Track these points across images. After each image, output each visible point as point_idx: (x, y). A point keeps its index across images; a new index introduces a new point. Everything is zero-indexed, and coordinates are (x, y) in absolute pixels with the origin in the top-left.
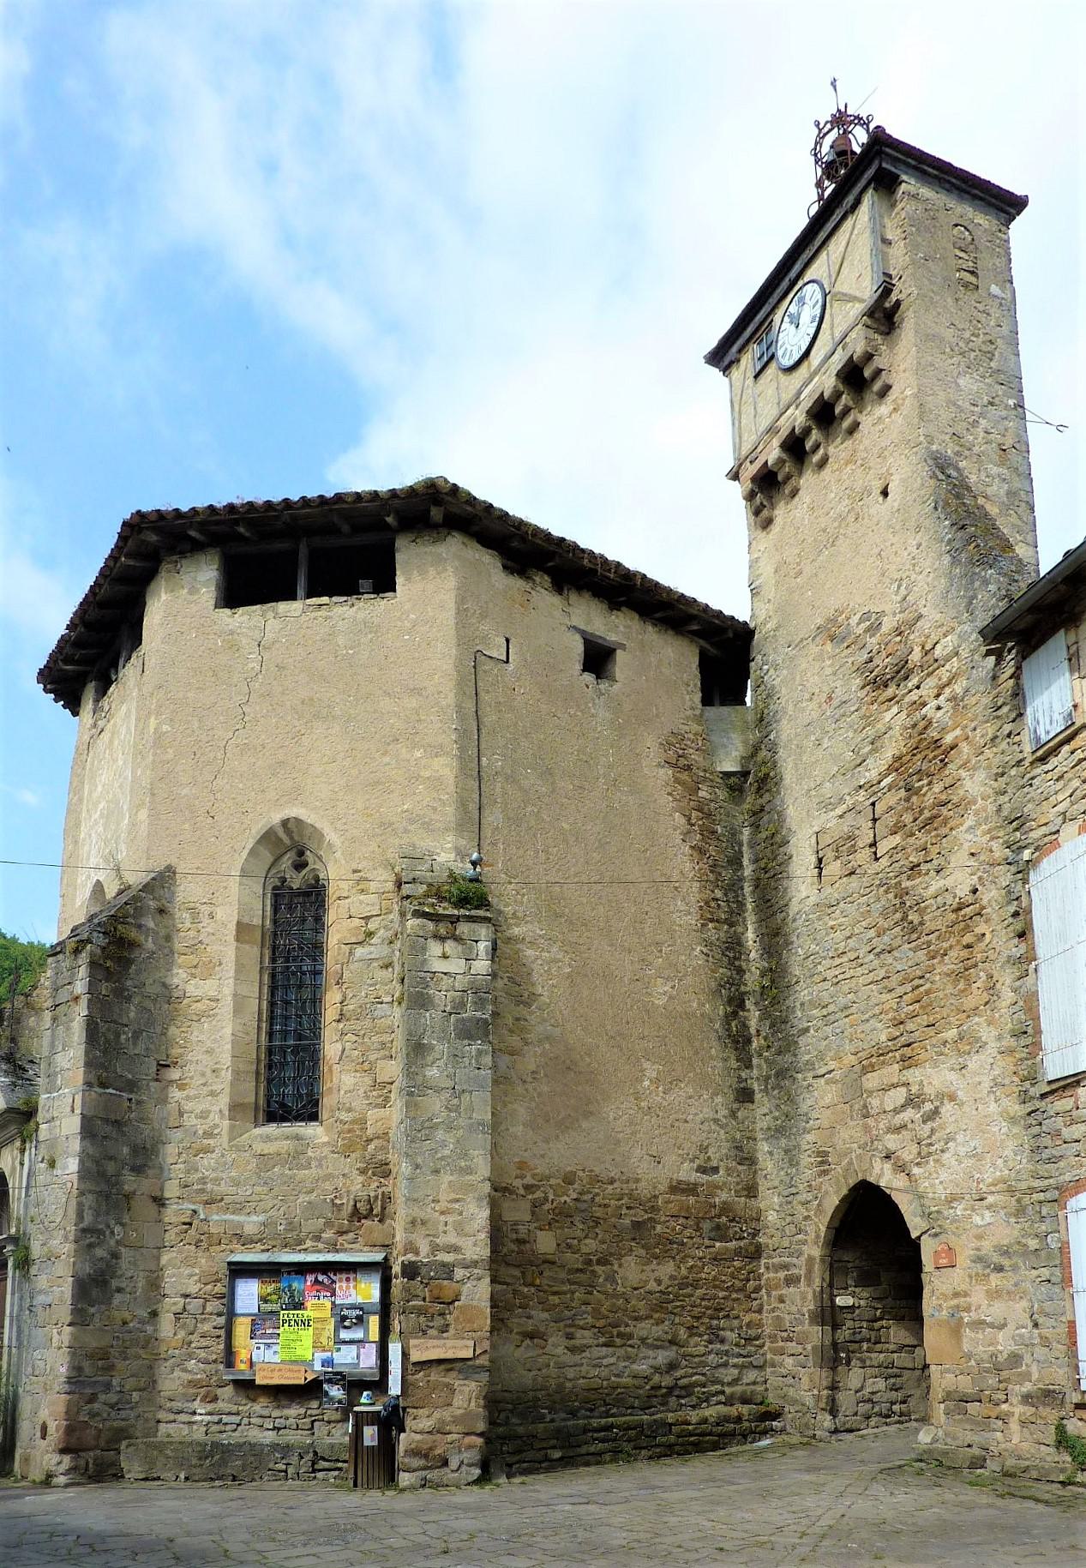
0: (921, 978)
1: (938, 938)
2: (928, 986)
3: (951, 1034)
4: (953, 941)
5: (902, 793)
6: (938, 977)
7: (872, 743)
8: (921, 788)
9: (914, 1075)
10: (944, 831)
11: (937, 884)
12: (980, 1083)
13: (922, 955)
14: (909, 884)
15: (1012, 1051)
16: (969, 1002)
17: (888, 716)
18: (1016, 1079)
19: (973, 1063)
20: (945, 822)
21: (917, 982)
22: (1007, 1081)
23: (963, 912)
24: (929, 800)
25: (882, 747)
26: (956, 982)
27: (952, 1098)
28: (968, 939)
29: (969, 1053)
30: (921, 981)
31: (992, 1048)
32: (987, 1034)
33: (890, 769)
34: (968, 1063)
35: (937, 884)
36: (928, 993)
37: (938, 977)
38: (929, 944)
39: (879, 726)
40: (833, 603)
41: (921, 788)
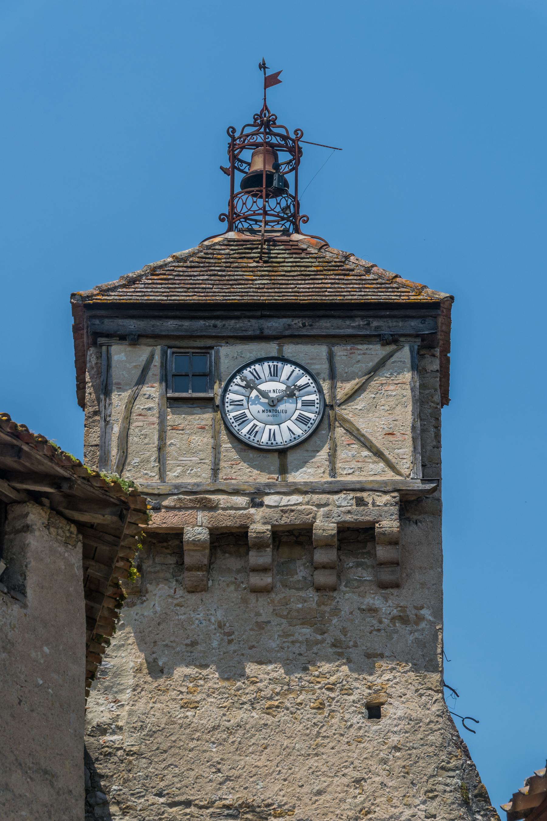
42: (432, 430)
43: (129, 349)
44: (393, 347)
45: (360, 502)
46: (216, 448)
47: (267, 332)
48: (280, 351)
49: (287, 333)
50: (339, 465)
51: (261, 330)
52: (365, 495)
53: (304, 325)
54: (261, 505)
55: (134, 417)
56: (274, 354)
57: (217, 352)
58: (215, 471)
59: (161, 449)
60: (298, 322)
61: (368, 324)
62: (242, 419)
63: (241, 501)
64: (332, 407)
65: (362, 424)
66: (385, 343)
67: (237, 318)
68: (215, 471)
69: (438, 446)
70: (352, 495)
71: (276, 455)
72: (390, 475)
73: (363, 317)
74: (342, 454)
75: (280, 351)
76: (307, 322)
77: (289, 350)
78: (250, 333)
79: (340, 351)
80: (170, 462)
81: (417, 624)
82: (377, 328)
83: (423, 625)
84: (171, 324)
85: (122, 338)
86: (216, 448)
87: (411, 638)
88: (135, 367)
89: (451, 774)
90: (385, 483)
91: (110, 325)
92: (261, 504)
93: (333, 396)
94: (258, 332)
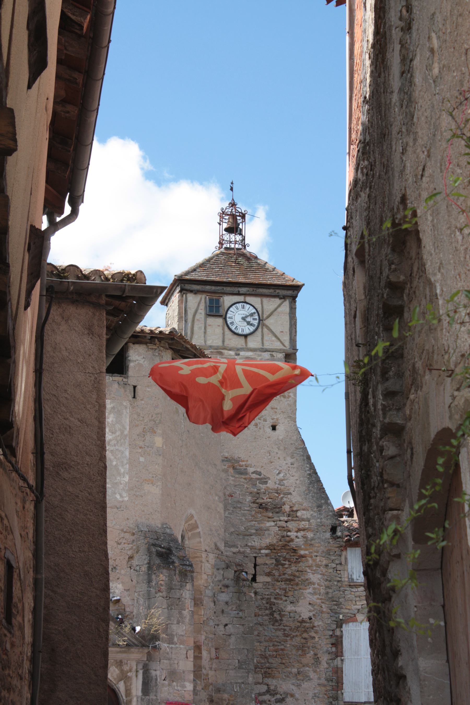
0: (280, 643)
1: (290, 630)
2: (282, 647)
3: (295, 670)
4: (297, 633)
5: (274, 561)
6: (288, 646)
7: (256, 530)
8: (285, 564)
9: (273, 683)
10: (294, 587)
11: (290, 608)
12: (307, 694)
13: (280, 633)
14: (275, 601)
15: (325, 686)
16: (304, 660)
17: (268, 524)
18: (326, 697)
19: (305, 685)
20: (297, 584)
21: (276, 643)
22: (321, 696)
23: (304, 624)
24: (289, 571)
25: (263, 535)
26: (298, 650)
27: (292, 696)
28: (305, 635)
29: (303, 680)
30: (278, 644)
31: (316, 681)
32: (312, 675)
33: (267, 548)
34: (302, 684)
35: (290, 608)
36: (282, 650)
37: (288, 646)
38: (285, 630)
39: (262, 525)
40: (242, 456)
41: (285, 564)
42: (294, 329)
43: (194, 295)
44: (283, 300)
45: (272, 356)
46: (224, 334)
47: (241, 292)
48: (245, 299)
49: (248, 293)
50: (264, 342)
51: (239, 291)
52: (273, 353)
53: (253, 290)
54: (239, 355)
55: (195, 321)
56: (243, 300)
57: (223, 299)
58: (223, 341)
59: (205, 333)
60: (251, 289)
61: (275, 291)
62: (232, 323)
63: (232, 353)
64: (262, 320)
65: (272, 328)
66: (281, 299)
67: (231, 286)
68: (223, 341)
69: (296, 336)
70: (269, 353)
71: (244, 337)
72: (282, 347)
73: (273, 289)
74: (266, 338)
75: (245, 299)
76: (255, 289)
77: (248, 299)
78: (235, 292)
79: (265, 300)
80: (208, 338)
81: (288, 398)
82: (278, 293)
83: (290, 399)
84: (208, 288)
85: (191, 291)
86: (224, 334)
87: (286, 403)
88: (196, 302)
89: (299, 450)
90: (280, 350)
91: (188, 287)
92: (239, 355)
93: (263, 317)
94: (237, 292)
